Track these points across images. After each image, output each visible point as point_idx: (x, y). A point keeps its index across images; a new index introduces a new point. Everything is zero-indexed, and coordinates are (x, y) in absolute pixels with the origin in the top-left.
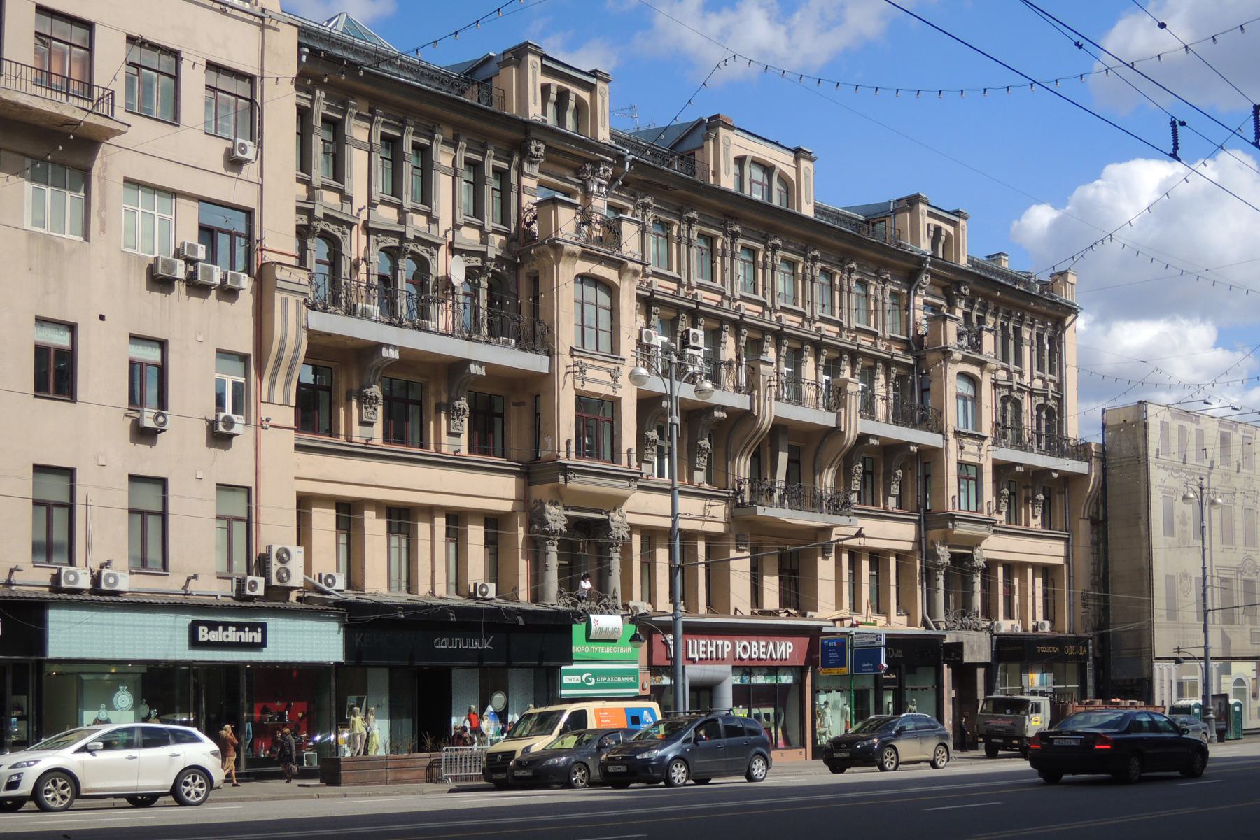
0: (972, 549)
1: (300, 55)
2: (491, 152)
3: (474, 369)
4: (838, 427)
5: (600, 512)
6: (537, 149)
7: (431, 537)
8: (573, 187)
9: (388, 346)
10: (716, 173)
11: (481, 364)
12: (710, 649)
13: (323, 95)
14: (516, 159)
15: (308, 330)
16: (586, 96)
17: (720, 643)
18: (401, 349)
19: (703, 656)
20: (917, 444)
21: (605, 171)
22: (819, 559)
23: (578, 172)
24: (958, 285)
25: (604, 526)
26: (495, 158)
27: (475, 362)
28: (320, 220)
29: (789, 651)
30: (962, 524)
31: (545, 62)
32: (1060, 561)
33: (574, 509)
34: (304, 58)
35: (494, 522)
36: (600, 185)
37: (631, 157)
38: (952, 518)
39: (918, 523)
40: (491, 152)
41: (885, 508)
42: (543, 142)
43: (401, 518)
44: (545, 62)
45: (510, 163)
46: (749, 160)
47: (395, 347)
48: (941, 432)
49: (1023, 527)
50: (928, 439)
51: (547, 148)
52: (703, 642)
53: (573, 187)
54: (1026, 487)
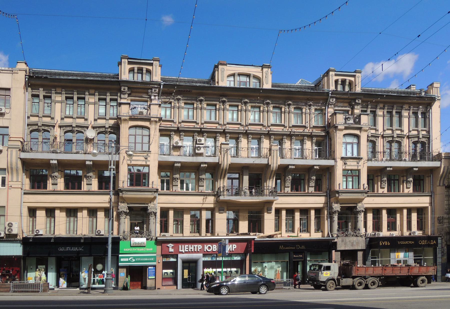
0: (357, 204)
1: (25, 78)
2: (108, 94)
3: (87, 163)
4: (268, 163)
5: (144, 204)
6: (124, 89)
7: (60, 216)
8: (146, 99)
9: (52, 160)
10: (218, 82)
11: (90, 161)
12: (190, 248)
13: (42, 89)
14: (119, 94)
15: (20, 158)
16: (150, 68)
17: (196, 246)
18: (58, 160)
19: (186, 251)
20: (318, 165)
21: (155, 91)
22: (266, 214)
23: (147, 93)
24: (355, 100)
25: (146, 209)
26: (110, 95)
27: (88, 160)
28: (41, 126)
29: (234, 248)
30: (343, 194)
31: (129, 60)
32: (427, 205)
33: (131, 204)
34: (27, 79)
35: (107, 211)
36: (155, 96)
37: (163, 84)
38: (338, 192)
39: (326, 196)
40: (108, 94)
41: (308, 192)
42: (126, 86)
43: (50, 212)
44: (129, 60)
45: (117, 96)
46: (236, 74)
47: (55, 160)
48: (334, 159)
49: (376, 192)
50: (329, 162)
51: (129, 88)
52: (186, 246)
53: (146, 99)
54: (403, 176)
